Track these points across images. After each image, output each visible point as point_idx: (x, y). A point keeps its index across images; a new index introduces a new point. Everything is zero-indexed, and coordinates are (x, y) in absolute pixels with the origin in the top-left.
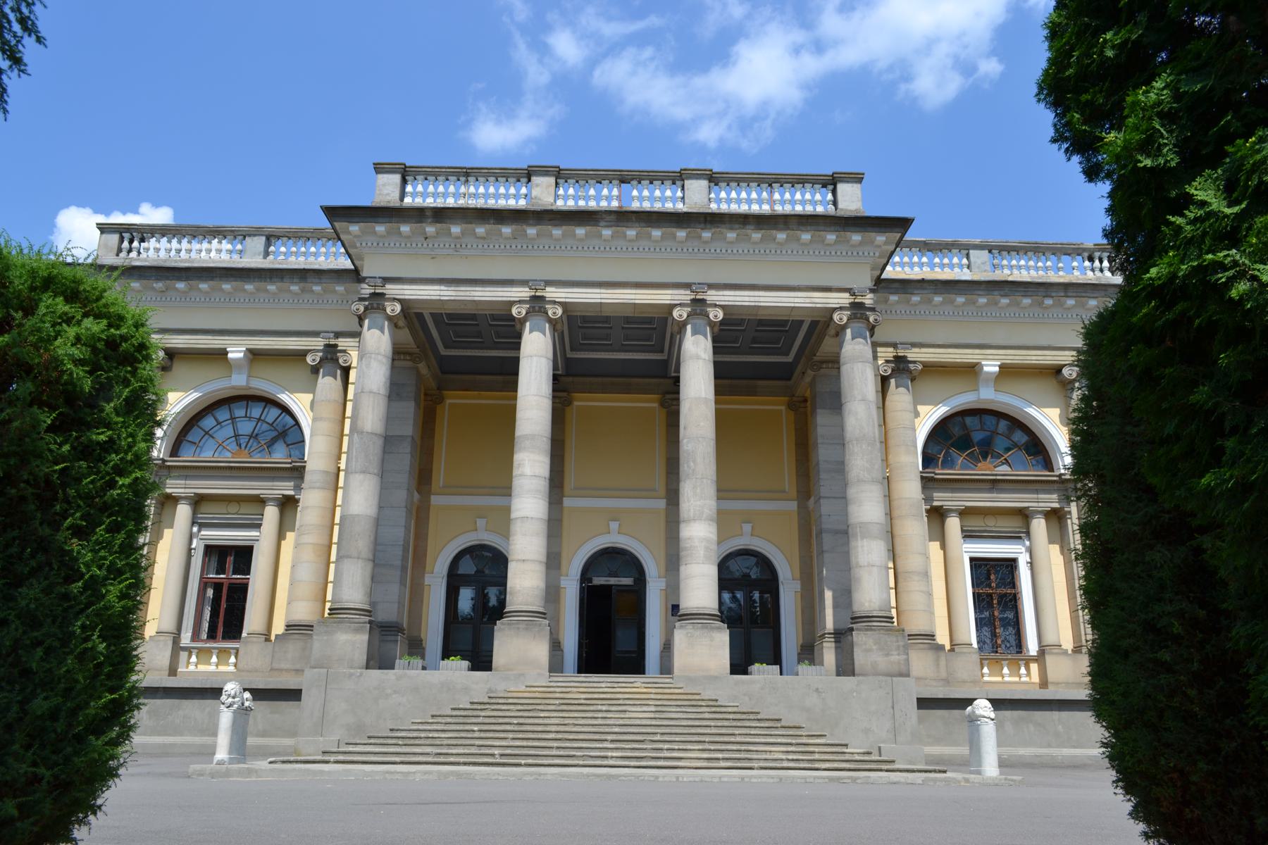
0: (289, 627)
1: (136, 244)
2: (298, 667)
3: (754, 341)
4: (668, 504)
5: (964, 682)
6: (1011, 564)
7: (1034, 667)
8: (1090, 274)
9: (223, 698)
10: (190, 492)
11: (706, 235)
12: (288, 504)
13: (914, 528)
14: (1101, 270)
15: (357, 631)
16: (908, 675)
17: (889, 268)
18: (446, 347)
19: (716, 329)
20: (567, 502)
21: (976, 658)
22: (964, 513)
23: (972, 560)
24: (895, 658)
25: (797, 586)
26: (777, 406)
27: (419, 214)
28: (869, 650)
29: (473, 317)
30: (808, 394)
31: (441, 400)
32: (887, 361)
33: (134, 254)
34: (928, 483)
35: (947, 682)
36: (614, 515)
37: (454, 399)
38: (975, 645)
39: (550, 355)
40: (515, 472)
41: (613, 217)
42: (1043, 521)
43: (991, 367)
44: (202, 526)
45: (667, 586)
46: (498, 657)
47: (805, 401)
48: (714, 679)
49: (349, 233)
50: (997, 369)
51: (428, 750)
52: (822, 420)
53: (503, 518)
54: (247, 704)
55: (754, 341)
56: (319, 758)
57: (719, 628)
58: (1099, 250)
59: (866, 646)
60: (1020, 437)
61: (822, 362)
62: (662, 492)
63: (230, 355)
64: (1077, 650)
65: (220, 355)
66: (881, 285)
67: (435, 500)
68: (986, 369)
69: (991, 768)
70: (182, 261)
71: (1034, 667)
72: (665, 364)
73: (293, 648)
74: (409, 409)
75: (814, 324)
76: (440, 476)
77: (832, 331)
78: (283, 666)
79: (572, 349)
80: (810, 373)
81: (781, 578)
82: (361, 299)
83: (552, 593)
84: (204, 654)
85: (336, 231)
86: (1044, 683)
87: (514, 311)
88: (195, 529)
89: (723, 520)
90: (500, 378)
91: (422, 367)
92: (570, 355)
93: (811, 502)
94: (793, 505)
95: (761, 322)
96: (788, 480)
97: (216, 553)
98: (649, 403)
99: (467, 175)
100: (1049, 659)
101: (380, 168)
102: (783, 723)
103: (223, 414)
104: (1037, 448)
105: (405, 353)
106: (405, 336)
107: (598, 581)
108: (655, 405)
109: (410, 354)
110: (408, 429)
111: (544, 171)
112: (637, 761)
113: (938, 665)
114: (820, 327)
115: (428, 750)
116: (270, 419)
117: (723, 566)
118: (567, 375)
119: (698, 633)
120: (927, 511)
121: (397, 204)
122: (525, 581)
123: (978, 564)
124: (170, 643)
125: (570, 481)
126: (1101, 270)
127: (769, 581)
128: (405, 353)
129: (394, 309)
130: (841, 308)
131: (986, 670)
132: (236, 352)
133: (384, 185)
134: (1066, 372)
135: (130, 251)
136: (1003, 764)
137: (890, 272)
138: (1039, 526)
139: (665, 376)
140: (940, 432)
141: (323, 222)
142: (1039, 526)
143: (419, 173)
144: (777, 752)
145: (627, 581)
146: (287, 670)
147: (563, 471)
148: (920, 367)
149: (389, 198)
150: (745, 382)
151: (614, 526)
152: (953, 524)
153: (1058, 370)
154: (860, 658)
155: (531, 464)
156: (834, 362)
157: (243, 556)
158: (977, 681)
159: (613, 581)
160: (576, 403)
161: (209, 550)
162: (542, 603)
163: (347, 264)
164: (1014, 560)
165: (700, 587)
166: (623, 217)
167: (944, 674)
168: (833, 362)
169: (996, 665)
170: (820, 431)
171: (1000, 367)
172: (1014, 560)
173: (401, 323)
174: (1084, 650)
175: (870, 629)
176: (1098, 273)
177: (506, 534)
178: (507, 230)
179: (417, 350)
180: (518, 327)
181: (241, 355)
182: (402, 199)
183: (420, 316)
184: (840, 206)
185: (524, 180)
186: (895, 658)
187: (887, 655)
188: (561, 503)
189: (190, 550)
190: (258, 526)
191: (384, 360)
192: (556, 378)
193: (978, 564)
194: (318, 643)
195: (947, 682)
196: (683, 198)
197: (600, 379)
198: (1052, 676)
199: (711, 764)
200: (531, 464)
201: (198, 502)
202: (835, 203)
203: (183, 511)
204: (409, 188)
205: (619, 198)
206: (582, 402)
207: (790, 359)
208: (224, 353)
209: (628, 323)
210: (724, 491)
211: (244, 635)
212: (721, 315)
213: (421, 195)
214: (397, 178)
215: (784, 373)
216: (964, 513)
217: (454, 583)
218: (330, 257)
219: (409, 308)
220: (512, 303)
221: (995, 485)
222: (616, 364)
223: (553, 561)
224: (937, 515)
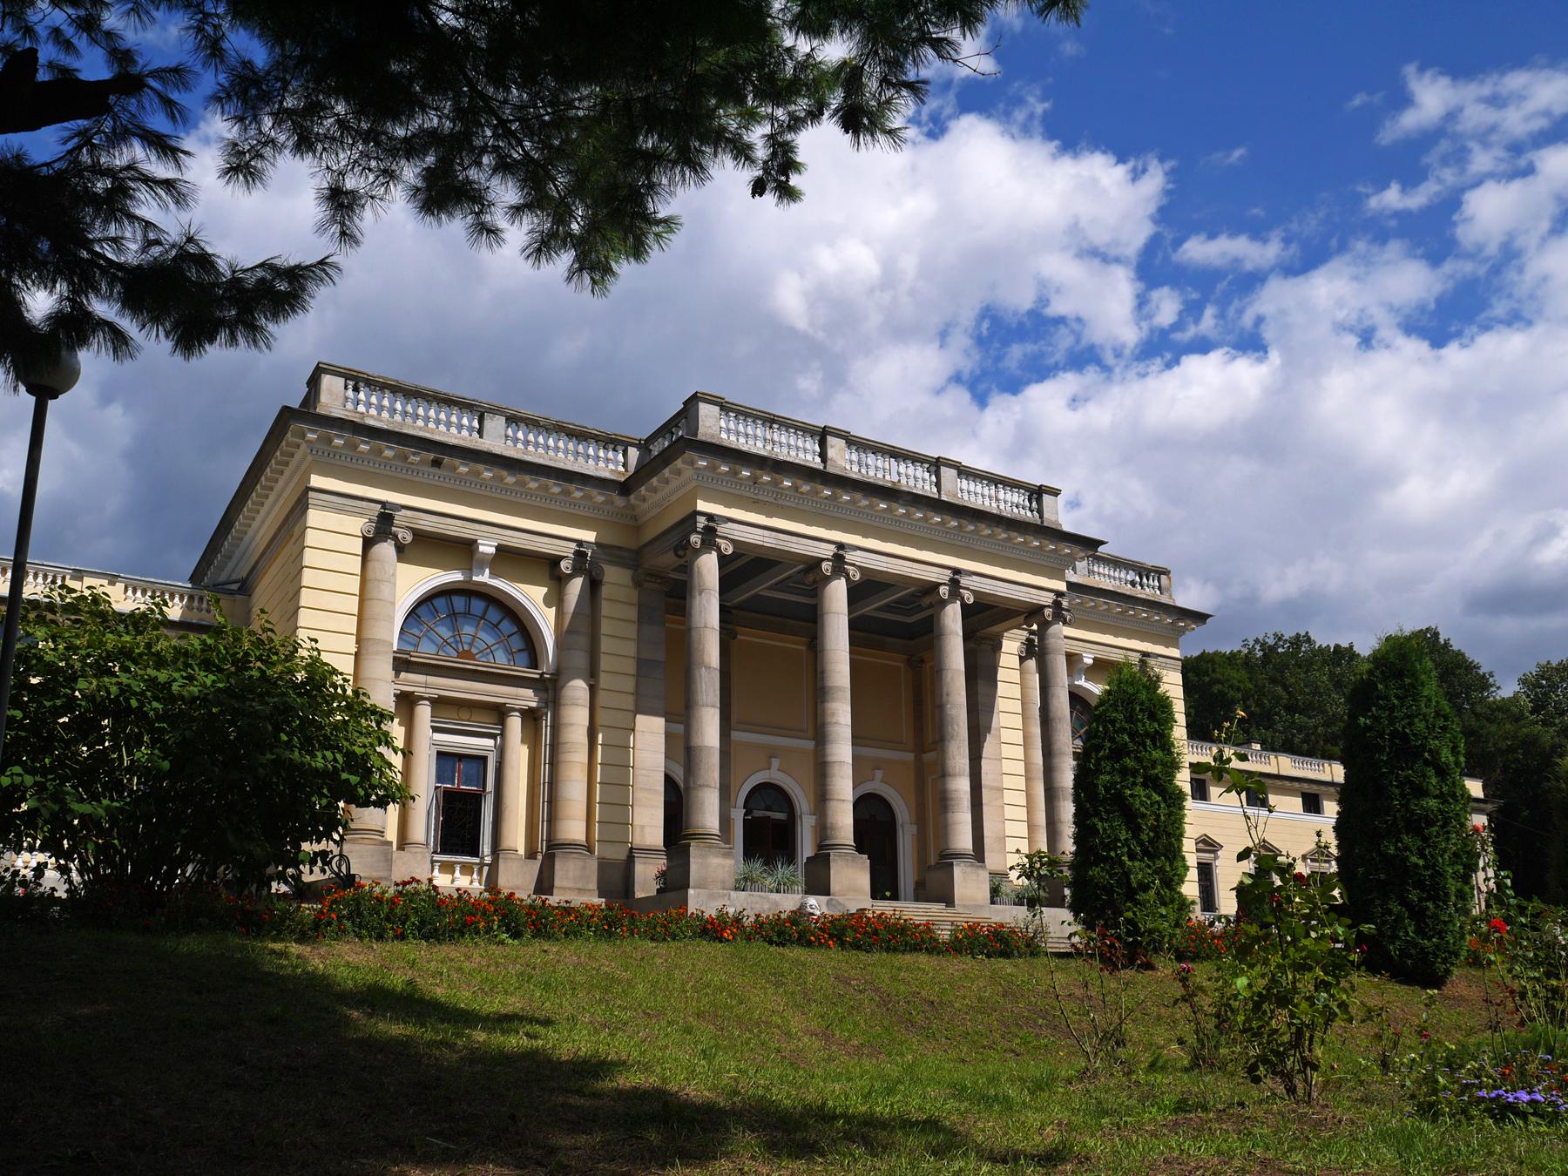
10: (434, 693)
25: (914, 829)
36: (772, 753)
46: (835, 885)
62: (810, 734)
65: (469, 546)
81: (899, 820)
94: (910, 756)
99: (773, 421)
107: (758, 814)
125: (734, 718)
132: (487, 548)
143: (732, 410)
155: (841, 714)
184: (1045, 516)
200: (841, 714)
210: (857, 739)
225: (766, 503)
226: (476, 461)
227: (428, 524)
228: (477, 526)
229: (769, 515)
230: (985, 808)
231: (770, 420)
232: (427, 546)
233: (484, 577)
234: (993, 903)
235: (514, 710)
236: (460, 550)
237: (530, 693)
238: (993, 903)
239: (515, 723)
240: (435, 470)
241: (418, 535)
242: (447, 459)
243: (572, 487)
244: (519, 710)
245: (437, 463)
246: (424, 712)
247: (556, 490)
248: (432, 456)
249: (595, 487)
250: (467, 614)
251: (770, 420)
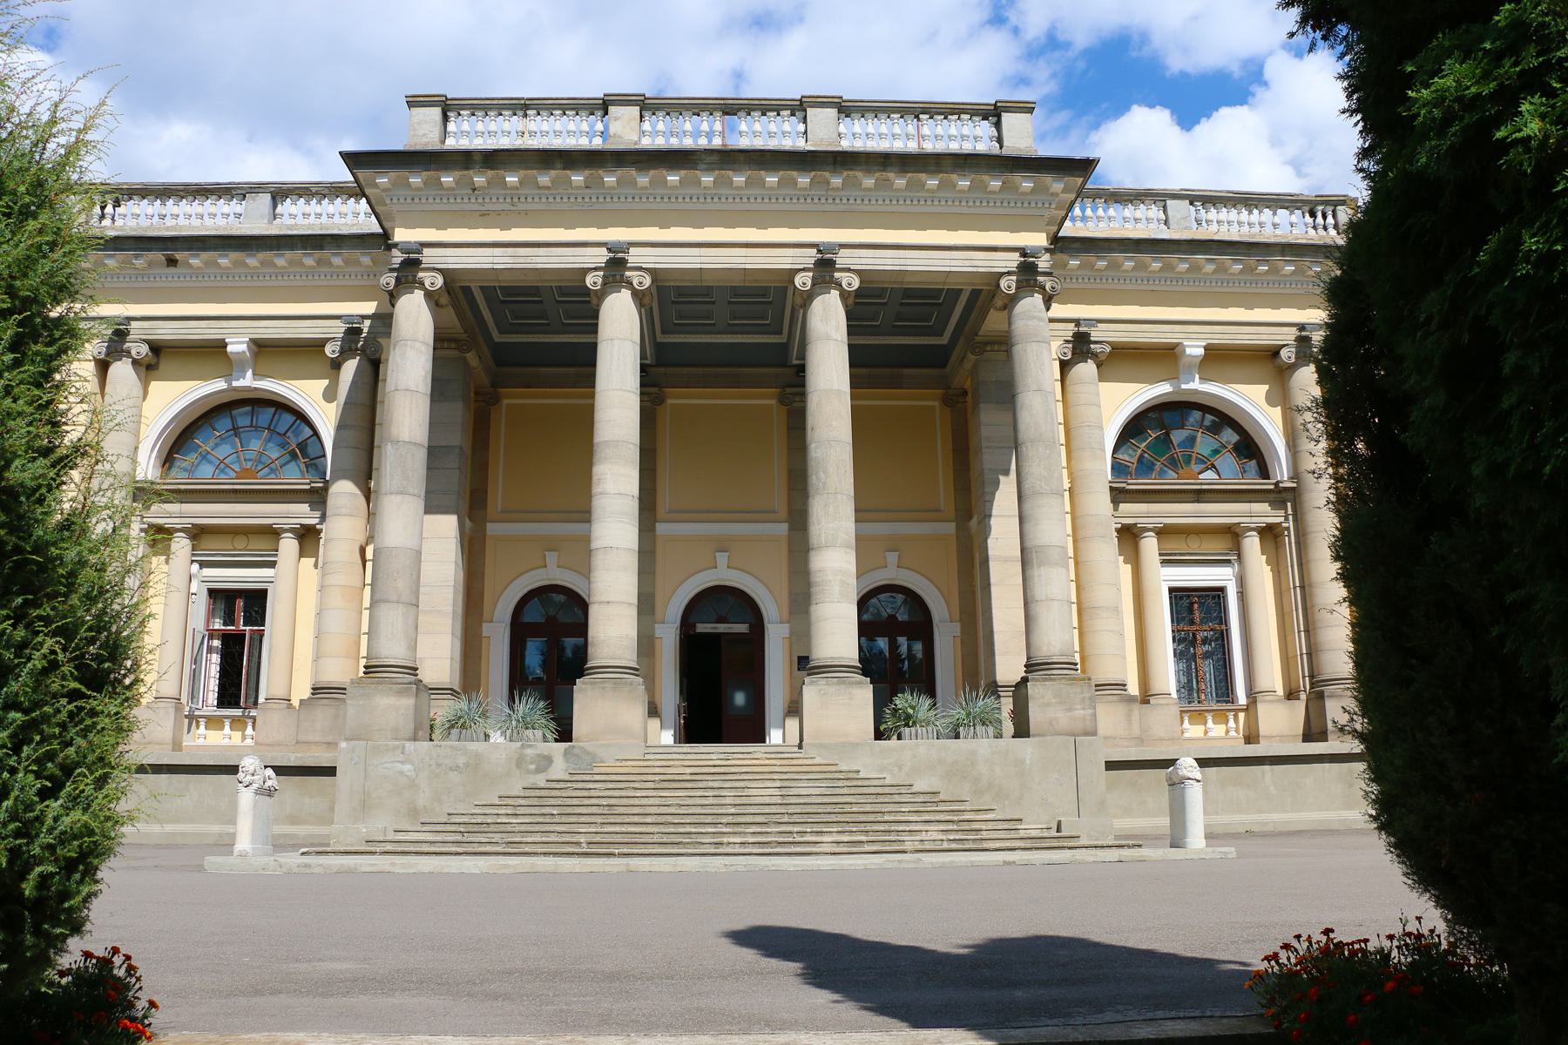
0: (316, 690)
1: (109, 209)
2: (330, 739)
3: (899, 317)
4: (791, 529)
5: (1162, 740)
6: (1218, 593)
7: (1242, 716)
8: (1312, 232)
9: (240, 775)
11: (837, 181)
12: (308, 537)
13: (1105, 552)
14: (1325, 228)
15: (400, 693)
16: (1094, 733)
17: (1067, 223)
18: (501, 332)
19: (851, 301)
20: (661, 528)
21: (1175, 710)
22: (1163, 532)
23: (1171, 590)
24: (1079, 713)
25: (956, 628)
26: (929, 401)
27: (465, 159)
28: (1048, 705)
29: (535, 291)
30: (968, 385)
31: (495, 400)
32: (1067, 342)
33: (107, 222)
34: (1119, 495)
35: (1140, 741)
37: (514, 399)
38: (1174, 695)
39: (637, 338)
40: (596, 489)
41: (715, 158)
42: (1257, 540)
43: (1195, 350)
44: (203, 565)
45: (792, 633)
47: (965, 393)
48: (851, 747)
49: (376, 186)
50: (1201, 351)
51: (497, 838)
52: (988, 420)
53: (582, 552)
54: (269, 783)
55: (899, 317)
56: (362, 848)
57: (860, 683)
58: (1322, 203)
59: (1044, 701)
60: (1230, 436)
61: (987, 343)
63: (230, 348)
64: (1291, 695)
66: (1059, 244)
67: (492, 528)
68: (1188, 351)
69: (1196, 839)
70: (167, 229)
71: (1242, 716)
72: (784, 348)
73: (323, 714)
74: (457, 411)
75: (975, 294)
76: (497, 497)
77: (999, 302)
78: (311, 738)
79: (663, 332)
80: (971, 357)
81: (936, 619)
82: (392, 270)
83: (646, 644)
84: (214, 723)
85: (359, 186)
86: (1251, 738)
87: (589, 280)
88: (195, 567)
89: (864, 547)
90: (572, 370)
91: (472, 358)
92: (661, 338)
93: (974, 522)
94: (950, 528)
95: (908, 293)
96: (944, 496)
97: (222, 598)
98: (766, 400)
100: (1262, 708)
101: (414, 102)
102: (942, 797)
103: (223, 424)
104: (1249, 448)
105: (449, 340)
106: (450, 315)
107: (702, 628)
108: (773, 402)
109: (455, 340)
110: (457, 438)
111: (624, 100)
112: (766, 849)
113: (1130, 722)
114: (981, 298)
115: (497, 838)
116: (281, 430)
117: (862, 604)
118: (657, 365)
119: (833, 689)
120: (1118, 531)
121: (437, 147)
122: (613, 628)
123: (1179, 596)
124: (172, 711)
125: (664, 502)
126: (1325, 228)
127: (920, 625)
128: (449, 340)
129: (434, 281)
130: (1009, 273)
131: (1186, 724)
132: (237, 346)
133: (419, 123)
134: (1284, 353)
135: (102, 217)
136: (1210, 836)
137: (1068, 229)
138: (1252, 543)
139: (785, 365)
140: (1133, 429)
141: (343, 174)
142: (1252, 543)
143: (464, 107)
144: (933, 833)
145: (742, 628)
146: (316, 743)
147: (655, 490)
148: (1108, 349)
149: (425, 140)
150: (887, 371)
151: (722, 558)
152: (1150, 545)
153: (1274, 352)
154: (1035, 714)
155: (616, 480)
156: (1004, 344)
157: (255, 602)
158: (1178, 738)
159: (722, 628)
160: (670, 401)
161: (213, 593)
162: (635, 657)
163: (373, 226)
164: (1222, 589)
165: (837, 632)
166: (728, 158)
167: (1136, 731)
168: (1000, 343)
169: (1198, 717)
170: (985, 431)
171: (1206, 348)
172: (1222, 589)
173: (444, 300)
174: (1303, 696)
175: (1049, 678)
176: (1321, 232)
177: (586, 572)
178: (577, 178)
179: (464, 336)
180: (594, 301)
181: (243, 347)
182: (443, 142)
183: (467, 290)
184: (1006, 143)
185: (599, 113)
186: (1079, 713)
187: (1070, 710)
188: (653, 530)
189: (190, 594)
190: (272, 565)
191: (423, 348)
192: (643, 368)
193: (1179, 596)
194: (353, 708)
195: (1140, 741)
196: (806, 132)
197: (700, 370)
198: (1264, 728)
199: (854, 848)
200: (616, 480)
201: (198, 534)
202: (1000, 140)
203: (181, 545)
204: (451, 127)
205: (722, 134)
206: (677, 399)
207: (944, 340)
208: (221, 345)
209: (736, 295)
211: (261, 700)
212: (856, 284)
213: (468, 134)
214: (436, 112)
215: (938, 358)
216: (1163, 532)
217: (520, 632)
218: (354, 217)
219: (453, 281)
220: (586, 271)
221: (1200, 496)
222: (723, 347)
223: (646, 605)
224: (1129, 536)
225: (499, 213)
226: (204, 249)
227: (166, 332)
228: (224, 323)
229: (505, 227)
230: (994, 589)
231: (522, 107)
232: (161, 358)
233: (247, 381)
234: (879, 735)
235: (286, 531)
236: (209, 353)
237: (305, 507)
238: (879, 735)
239: (289, 545)
240: (172, 270)
241: (157, 348)
242: (178, 255)
243: (325, 253)
244: (291, 530)
245: (172, 262)
246: (181, 545)
247: (309, 261)
248: (159, 256)
249: (355, 247)
250: (255, 428)
251: (522, 107)
